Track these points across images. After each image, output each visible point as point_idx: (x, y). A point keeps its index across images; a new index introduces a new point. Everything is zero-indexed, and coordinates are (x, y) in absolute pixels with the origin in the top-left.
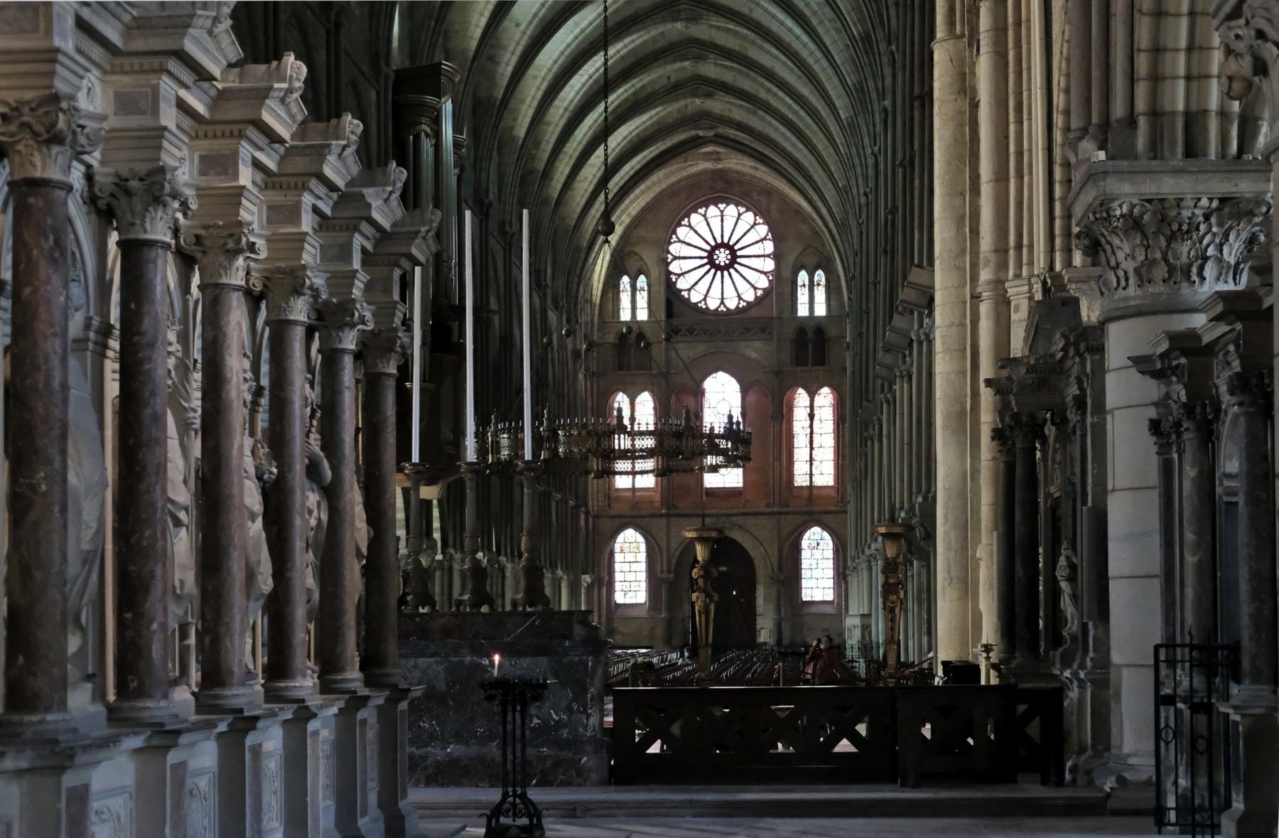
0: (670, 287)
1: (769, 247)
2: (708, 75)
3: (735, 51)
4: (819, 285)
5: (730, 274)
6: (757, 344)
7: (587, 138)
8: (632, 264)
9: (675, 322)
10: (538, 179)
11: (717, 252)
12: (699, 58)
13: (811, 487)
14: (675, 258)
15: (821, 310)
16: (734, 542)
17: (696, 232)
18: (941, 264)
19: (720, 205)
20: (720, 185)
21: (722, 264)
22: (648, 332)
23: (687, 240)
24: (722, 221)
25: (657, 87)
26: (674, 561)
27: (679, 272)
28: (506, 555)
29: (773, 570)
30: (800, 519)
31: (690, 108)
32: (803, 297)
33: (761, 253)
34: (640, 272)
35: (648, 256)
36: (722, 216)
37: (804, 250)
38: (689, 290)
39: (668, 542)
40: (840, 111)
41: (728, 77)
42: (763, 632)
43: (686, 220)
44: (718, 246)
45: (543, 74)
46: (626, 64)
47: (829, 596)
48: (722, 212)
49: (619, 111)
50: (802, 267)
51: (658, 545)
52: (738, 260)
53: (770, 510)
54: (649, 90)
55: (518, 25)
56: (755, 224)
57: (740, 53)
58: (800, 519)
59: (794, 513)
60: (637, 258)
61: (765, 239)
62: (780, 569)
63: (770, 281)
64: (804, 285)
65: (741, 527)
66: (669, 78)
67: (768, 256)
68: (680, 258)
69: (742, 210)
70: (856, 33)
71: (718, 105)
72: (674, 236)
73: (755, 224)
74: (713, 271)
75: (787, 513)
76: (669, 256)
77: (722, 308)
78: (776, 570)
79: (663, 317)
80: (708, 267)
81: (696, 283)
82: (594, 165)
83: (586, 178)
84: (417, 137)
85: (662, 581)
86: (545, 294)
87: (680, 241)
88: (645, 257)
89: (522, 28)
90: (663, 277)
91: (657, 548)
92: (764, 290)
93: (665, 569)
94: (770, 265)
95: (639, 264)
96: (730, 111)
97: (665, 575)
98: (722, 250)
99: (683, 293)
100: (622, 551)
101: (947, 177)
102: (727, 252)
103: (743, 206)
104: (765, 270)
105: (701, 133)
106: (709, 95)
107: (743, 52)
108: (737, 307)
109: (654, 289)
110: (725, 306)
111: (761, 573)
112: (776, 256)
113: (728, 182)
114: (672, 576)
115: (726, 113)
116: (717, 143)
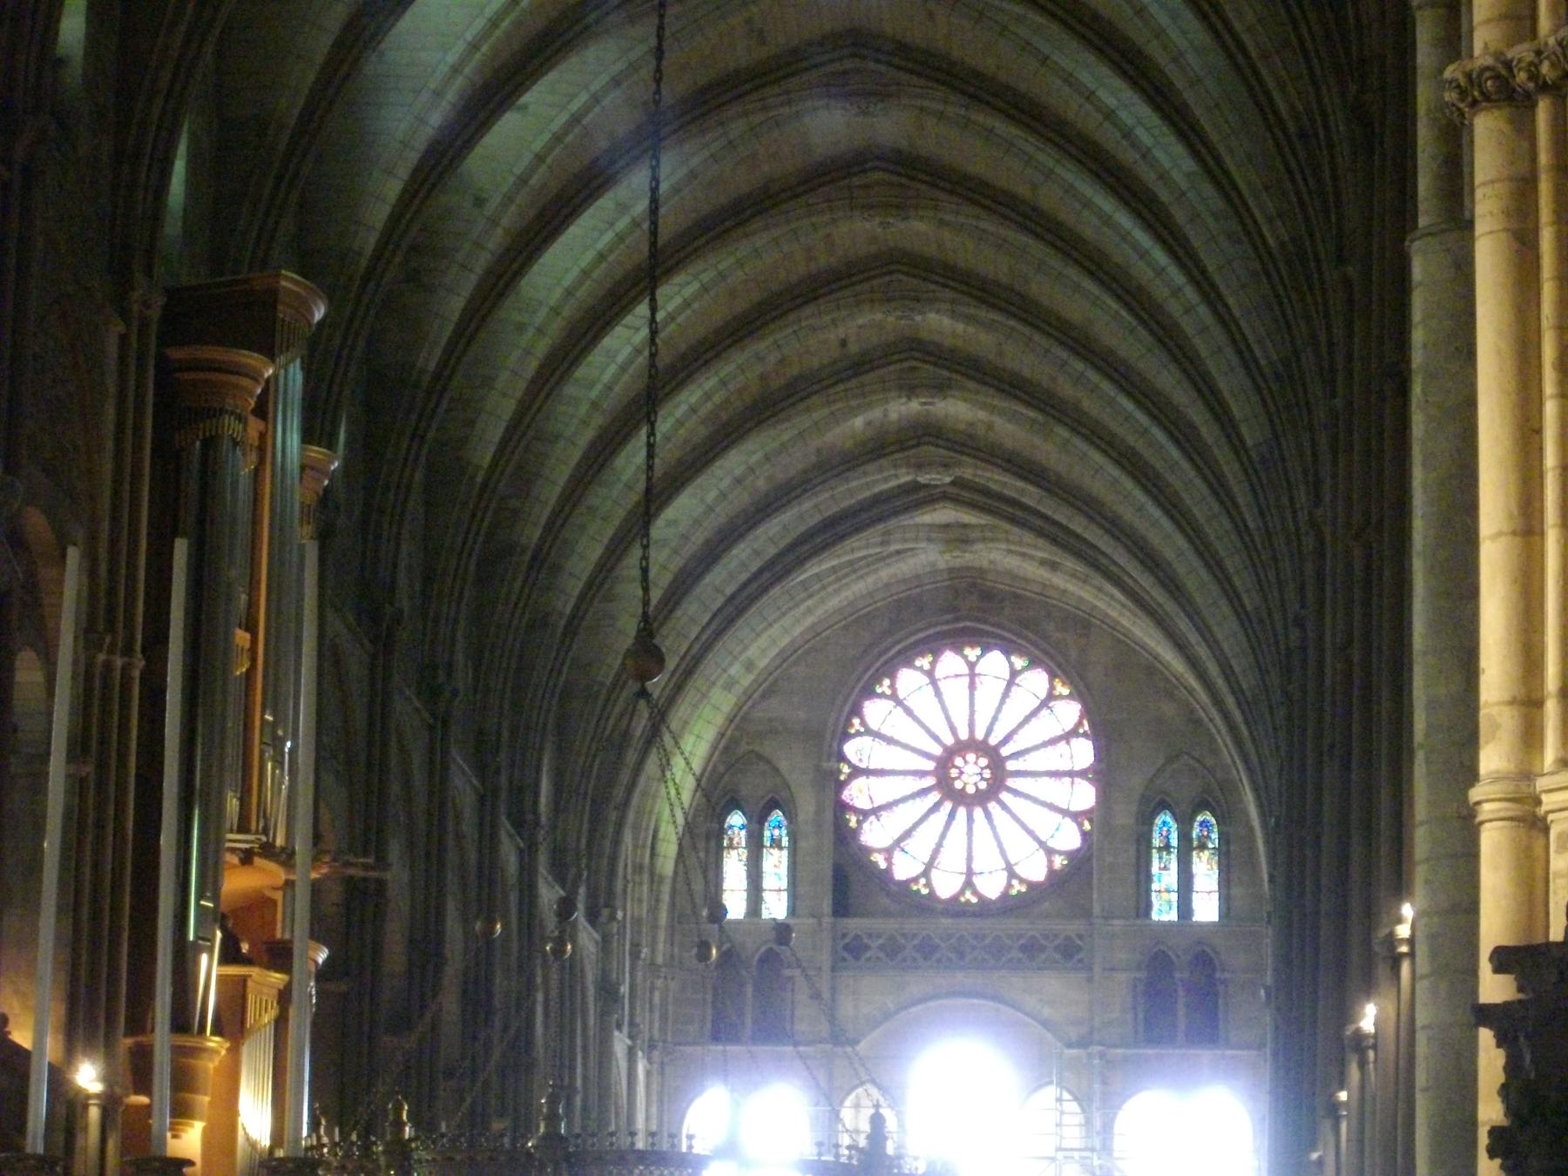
4: (1202, 847)
8: (753, 785)
9: (854, 924)
10: (524, 568)
14: (857, 772)
18: (1428, 761)
23: (885, 731)
24: (972, 686)
32: (1164, 877)
33: (1066, 767)
34: (773, 804)
35: (792, 764)
37: (1170, 760)
40: (1244, 429)
44: (960, 748)
48: (972, 666)
50: (1163, 806)
52: (1010, 782)
60: (762, 766)
63: (1084, 834)
66: (844, 343)
69: (1019, 662)
70: (1271, 242)
74: (948, 806)
76: (846, 769)
80: (934, 797)
81: (907, 834)
88: (783, 766)
90: (829, 815)
92: (1070, 855)
94: (1085, 796)
102: (984, 762)
103: (1021, 652)
106: (940, 388)
110: (975, 893)
112: (1103, 774)
113: (988, 596)
116: (956, 501)
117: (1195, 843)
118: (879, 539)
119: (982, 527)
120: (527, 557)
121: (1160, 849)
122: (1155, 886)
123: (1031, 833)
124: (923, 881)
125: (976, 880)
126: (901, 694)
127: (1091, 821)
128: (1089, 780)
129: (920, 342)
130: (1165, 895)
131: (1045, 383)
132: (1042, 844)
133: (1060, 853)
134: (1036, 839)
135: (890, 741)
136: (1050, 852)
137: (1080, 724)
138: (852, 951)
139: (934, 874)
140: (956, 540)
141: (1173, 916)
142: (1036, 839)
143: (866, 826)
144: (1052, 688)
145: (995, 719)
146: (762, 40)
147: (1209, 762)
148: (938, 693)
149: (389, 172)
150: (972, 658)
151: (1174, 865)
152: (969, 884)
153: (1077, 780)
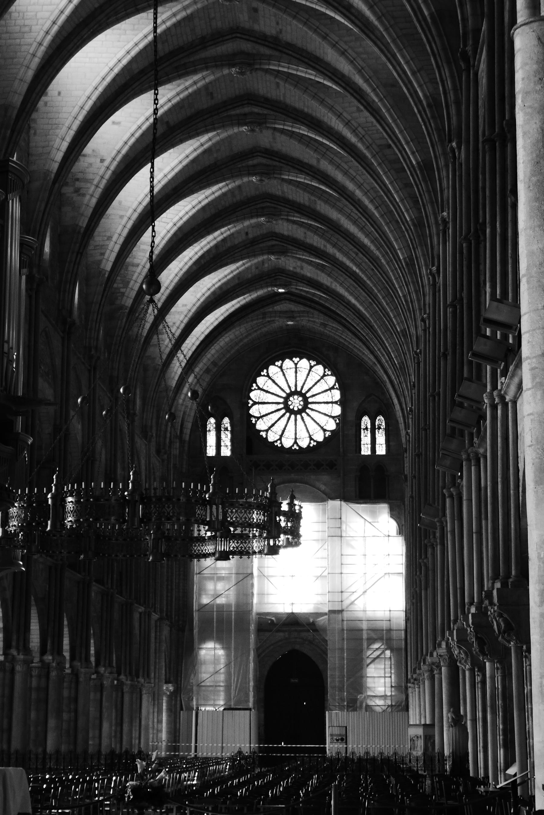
1: (337, 395)
2: (282, 232)
3: (304, 205)
4: (379, 428)
5: (302, 418)
6: (325, 478)
7: (173, 284)
10: (126, 314)
11: (291, 399)
14: (255, 403)
15: (381, 450)
17: (274, 381)
18: (528, 282)
19: (294, 359)
21: (296, 409)
23: (265, 388)
24: (296, 372)
25: (236, 242)
27: (258, 415)
28: (80, 660)
31: (266, 265)
32: (366, 439)
33: (330, 400)
36: (296, 368)
38: (267, 431)
41: (299, 233)
43: (265, 371)
45: (128, 214)
48: (296, 364)
52: (310, 406)
55: (102, 161)
56: (324, 375)
61: (333, 388)
63: (337, 424)
64: (366, 429)
66: (247, 234)
67: (336, 403)
68: (259, 403)
69: (313, 363)
70: (414, 163)
72: (254, 385)
73: (324, 375)
76: (251, 402)
77: (295, 447)
80: (283, 411)
82: (182, 312)
83: (174, 323)
86: (133, 421)
87: (259, 388)
89: (106, 163)
94: (337, 410)
96: (302, 268)
98: (296, 397)
99: (261, 433)
101: (534, 179)
102: (301, 399)
104: (333, 415)
108: (309, 446)
110: (298, 445)
115: (298, 270)
116: (290, 300)
117: (377, 427)
118: (262, 316)
119: (299, 312)
120: (127, 311)
121: (364, 429)
122: (362, 443)
123: (318, 424)
124: (279, 442)
125: (298, 441)
126: (271, 375)
127: (339, 419)
128: (339, 405)
129: (275, 233)
130: (366, 445)
131: (322, 247)
132: (322, 428)
133: (328, 431)
134: (320, 426)
135: (267, 392)
136: (325, 430)
137: (335, 385)
139: (283, 439)
140: (290, 317)
141: (369, 453)
142: (320, 426)
143: (258, 422)
144: (325, 372)
145: (304, 384)
146: (212, 98)
148: (284, 375)
150: (296, 362)
151: (369, 435)
152: (296, 442)
153: (334, 405)
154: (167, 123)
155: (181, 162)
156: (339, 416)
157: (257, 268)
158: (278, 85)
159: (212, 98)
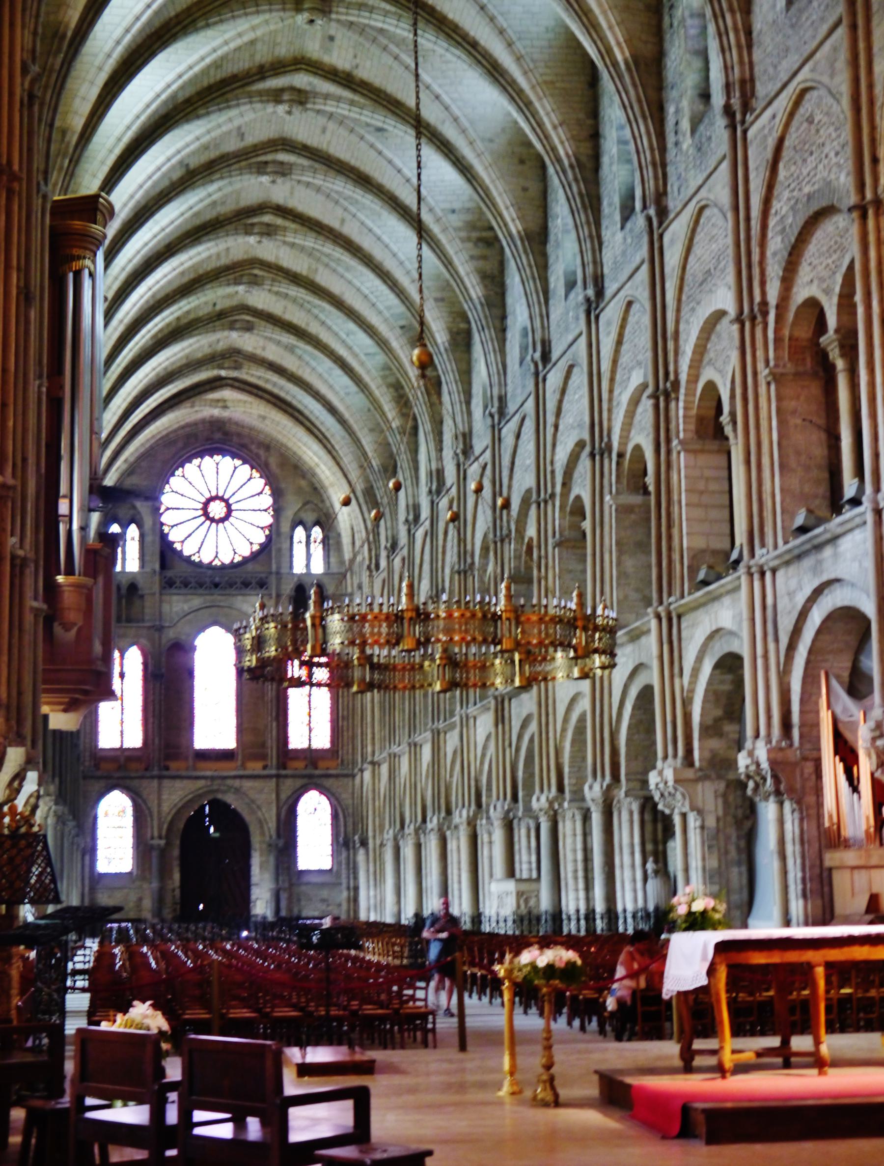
0: (164, 537)
3: (301, 275)
9: (169, 574)
12: (255, 282)
13: (309, 750)
15: (318, 567)
16: (227, 806)
20: (218, 436)
22: (141, 583)
25: (201, 313)
26: (165, 826)
29: (271, 837)
30: (299, 782)
31: (221, 344)
34: (132, 521)
39: (159, 805)
42: (259, 903)
46: (186, 279)
47: (326, 864)
49: (160, 336)
50: (301, 523)
51: (149, 809)
53: (266, 772)
54: (192, 316)
57: (306, 277)
58: (299, 782)
59: (293, 776)
62: (279, 835)
65: (237, 791)
66: (215, 305)
69: (238, 462)
71: (248, 342)
75: (286, 776)
78: (274, 836)
79: (157, 567)
84: (78, 275)
85: (152, 848)
90: (158, 526)
91: (147, 812)
93: (156, 834)
95: (132, 512)
97: (156, 842)
100: (106, 815)
103: (239, 458)
105: (223, 373)
106: (249, 328)
107: (311, 277)
109: (149, 539)
111: (256, 840)
112: (277, 510)
113: (226, 434)
114: (162, 842)
115: (259, 352)
116: (232, 387)
138: (169, 584)
141: (304, 571)
146: (242, 139)
147: (321, 505)
149: (94, 176)
154: (187, 165)
155: (182, 214)
156: (271, 526)
157: (210, 346)
158: (324, 130)
159: (242, 139)
